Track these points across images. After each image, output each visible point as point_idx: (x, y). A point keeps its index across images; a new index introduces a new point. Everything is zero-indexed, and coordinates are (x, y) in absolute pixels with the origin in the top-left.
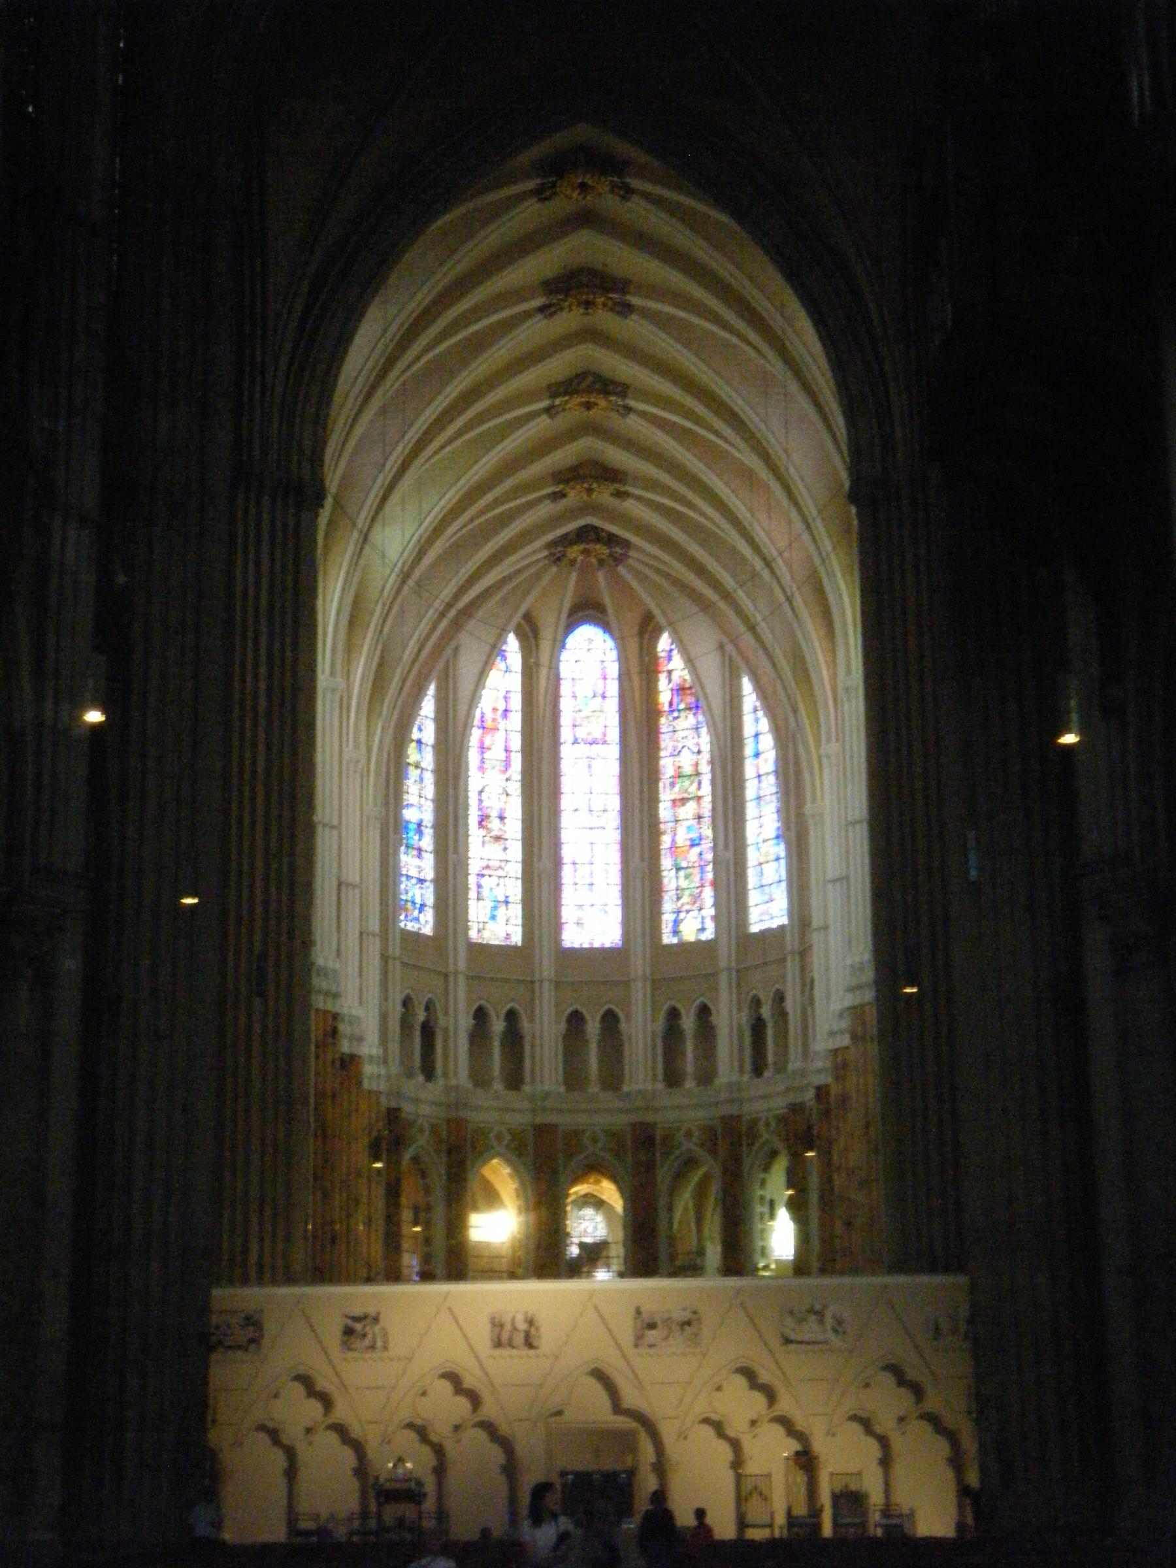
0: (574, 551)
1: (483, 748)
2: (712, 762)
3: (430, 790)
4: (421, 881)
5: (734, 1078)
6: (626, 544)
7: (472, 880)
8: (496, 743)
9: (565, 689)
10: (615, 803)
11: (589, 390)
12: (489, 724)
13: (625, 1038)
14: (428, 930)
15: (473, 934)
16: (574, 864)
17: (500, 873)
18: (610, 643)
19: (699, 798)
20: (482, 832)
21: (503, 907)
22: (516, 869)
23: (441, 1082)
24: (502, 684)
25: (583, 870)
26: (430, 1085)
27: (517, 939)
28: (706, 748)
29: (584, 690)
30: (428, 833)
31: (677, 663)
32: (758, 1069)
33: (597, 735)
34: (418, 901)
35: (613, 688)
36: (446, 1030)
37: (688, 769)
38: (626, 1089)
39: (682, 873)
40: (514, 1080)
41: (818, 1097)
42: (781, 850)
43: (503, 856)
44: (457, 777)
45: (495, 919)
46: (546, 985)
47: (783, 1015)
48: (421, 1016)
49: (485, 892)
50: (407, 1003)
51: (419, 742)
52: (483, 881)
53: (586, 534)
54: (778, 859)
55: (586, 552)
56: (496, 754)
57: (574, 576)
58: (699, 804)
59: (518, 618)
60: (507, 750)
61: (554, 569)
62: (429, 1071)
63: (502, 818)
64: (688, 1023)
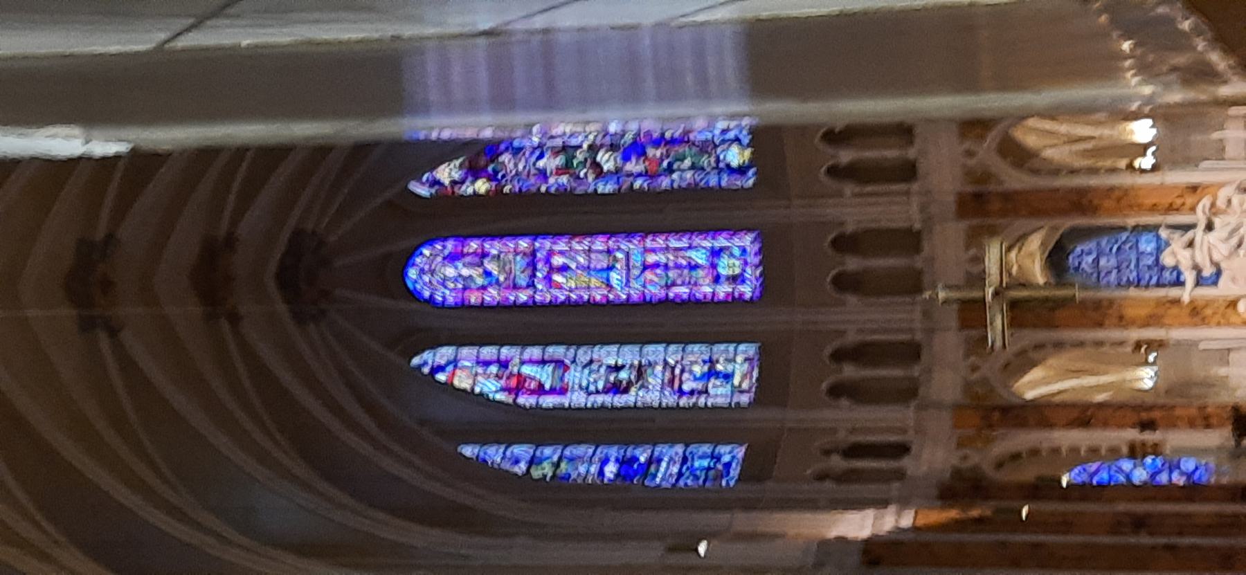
3: (584, 450)
6: (298, 234)
7: (684, 402)
9: (474, 298)
10: (599, 244)
14: (740, 452)
15: (745, 399)
16: (668, 287)
17: (677, 371)
20: (633, 390)
22: (673, 354)
24: (471, 372)
26: (914, 449)
31: (447, 173)
33: (520, 263)
34: (705, 463)
36: (853, 431)
37: (559, 161)
38: (917, 226)
40: (911, 352)
43: (659, 368)
45: (730, 374)
48: (837, 462)
49: (698, 386)
50: (822, 477)
52: (686, 387)
53: (288, 280)
56: (545, 375)
59: (392, 356)
60: (543, 362)
62: (902, 450)
63: (617, 368)
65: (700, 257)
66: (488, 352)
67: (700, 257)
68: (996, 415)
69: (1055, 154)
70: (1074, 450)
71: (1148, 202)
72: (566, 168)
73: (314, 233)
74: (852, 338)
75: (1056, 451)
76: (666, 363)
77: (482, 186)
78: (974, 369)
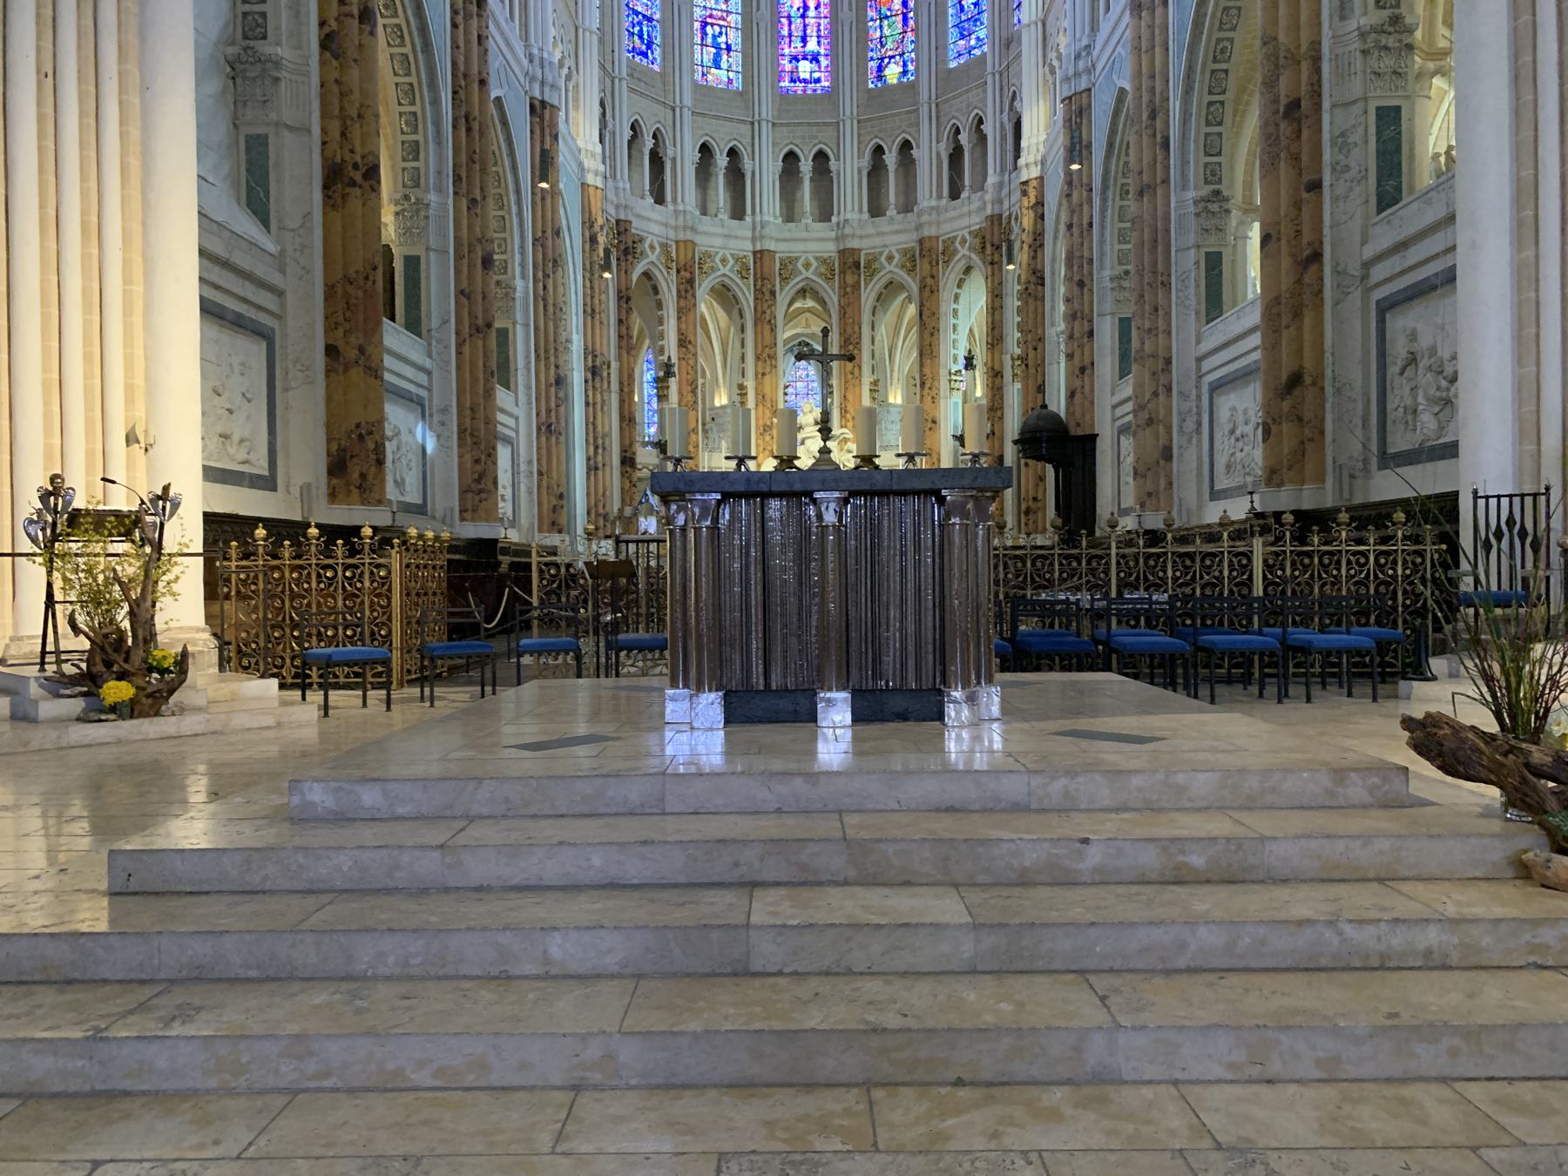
4: (650, 20)
5: (933, 203)
13: (834, 175)
23: (671, 207)
27: (738, 84)
32: (955, 194)
36: (674, 160)
38: (834, 219)
40: (738, 213)
41: (1025, 193)
46: (764, 124)
47: (982, 138)
49: (709, 40)
50: (633, 128)
52: (709, 29)
62: (660, 199)
64: (891, 159)
65: (812, 45)
67: (812, 45)
68: (688, 275)
69: (883, 332)
70: (662, 336)
71: (850, 397)
74: (747, 165)
75: (661, 322)
76: (728, 13)
78: (723, 261)
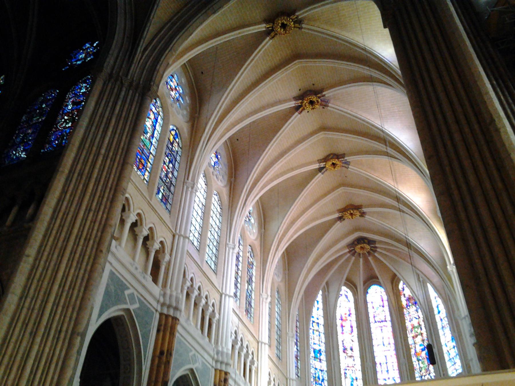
0: (358, 249)
1: (342, 326)
2: (423, 321)
4: (321, 371)
7: (342, 372)
8: (347, 325)
10: (392, 341)
11: (331, 159)
12: (344, 318)
18: (383, 290)
19: (422, 334)
20: (345, 354)
21: (355, 381)
22: (359, 366)
25: (384, 366)
28: (421, 316)
29: (376, 305)
30: (323, 354)
31: (407, 292)
34: (321, 378)
35: (386, 303)
37: (416, 325)
39: (420, 362)
42: (454, 344)
44: (332, 334)
49: (348, 376)
51: (318, 323)
52: (346, 371)
53: (360, 240)
54: (454, 347)
55: (362, 248)
57: (361, 260)
58: (422, 336)
60: (352, 327)
61: (353, 258)
63: (352, 349)
66: (353, 312)
72: (413, 327)
73: (376, 247)
77: (404, 303)
